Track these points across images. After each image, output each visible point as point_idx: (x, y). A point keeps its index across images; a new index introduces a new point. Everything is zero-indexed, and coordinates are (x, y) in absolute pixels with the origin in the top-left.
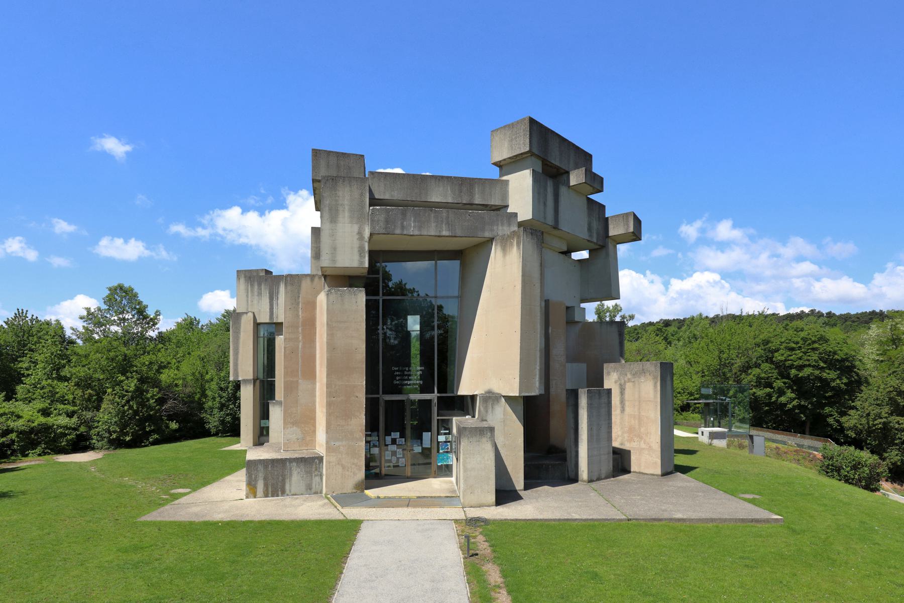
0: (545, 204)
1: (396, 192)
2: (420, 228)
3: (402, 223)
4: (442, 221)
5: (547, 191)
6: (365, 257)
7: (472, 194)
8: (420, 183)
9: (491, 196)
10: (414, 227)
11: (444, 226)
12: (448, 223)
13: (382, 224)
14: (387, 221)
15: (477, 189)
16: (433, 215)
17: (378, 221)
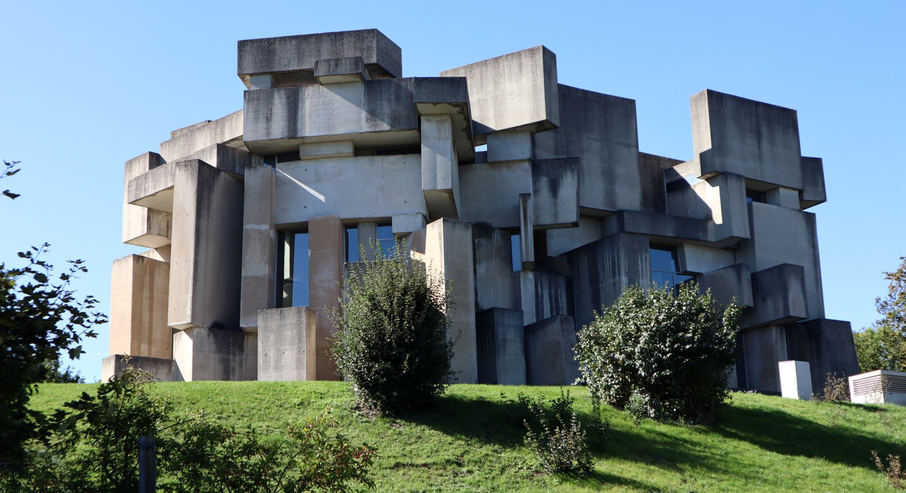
0: (268, 119)
1: (175, 155)
2: (155, 186)
3: (145, 187)
4: (168, 174)
5: (272, 104)
6: (145, 225)
7: (223, 132)
8: (190, 140)
9: (237, 128)
10: (152, 187)
11: (169, 178)
12: (172, 175)
13: (133, 193)
14: (137, 189)
15: (226, 127)
16: (162, 171)
17: (132, 191)
